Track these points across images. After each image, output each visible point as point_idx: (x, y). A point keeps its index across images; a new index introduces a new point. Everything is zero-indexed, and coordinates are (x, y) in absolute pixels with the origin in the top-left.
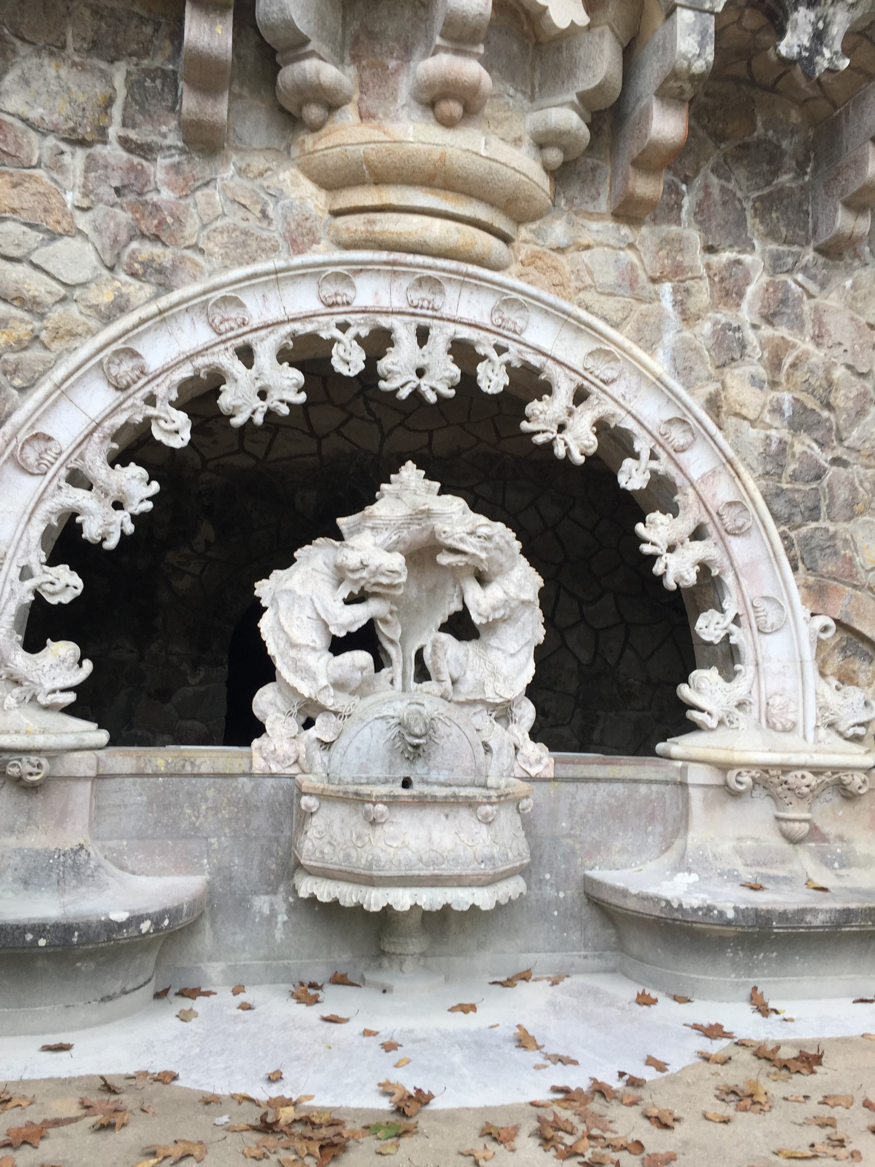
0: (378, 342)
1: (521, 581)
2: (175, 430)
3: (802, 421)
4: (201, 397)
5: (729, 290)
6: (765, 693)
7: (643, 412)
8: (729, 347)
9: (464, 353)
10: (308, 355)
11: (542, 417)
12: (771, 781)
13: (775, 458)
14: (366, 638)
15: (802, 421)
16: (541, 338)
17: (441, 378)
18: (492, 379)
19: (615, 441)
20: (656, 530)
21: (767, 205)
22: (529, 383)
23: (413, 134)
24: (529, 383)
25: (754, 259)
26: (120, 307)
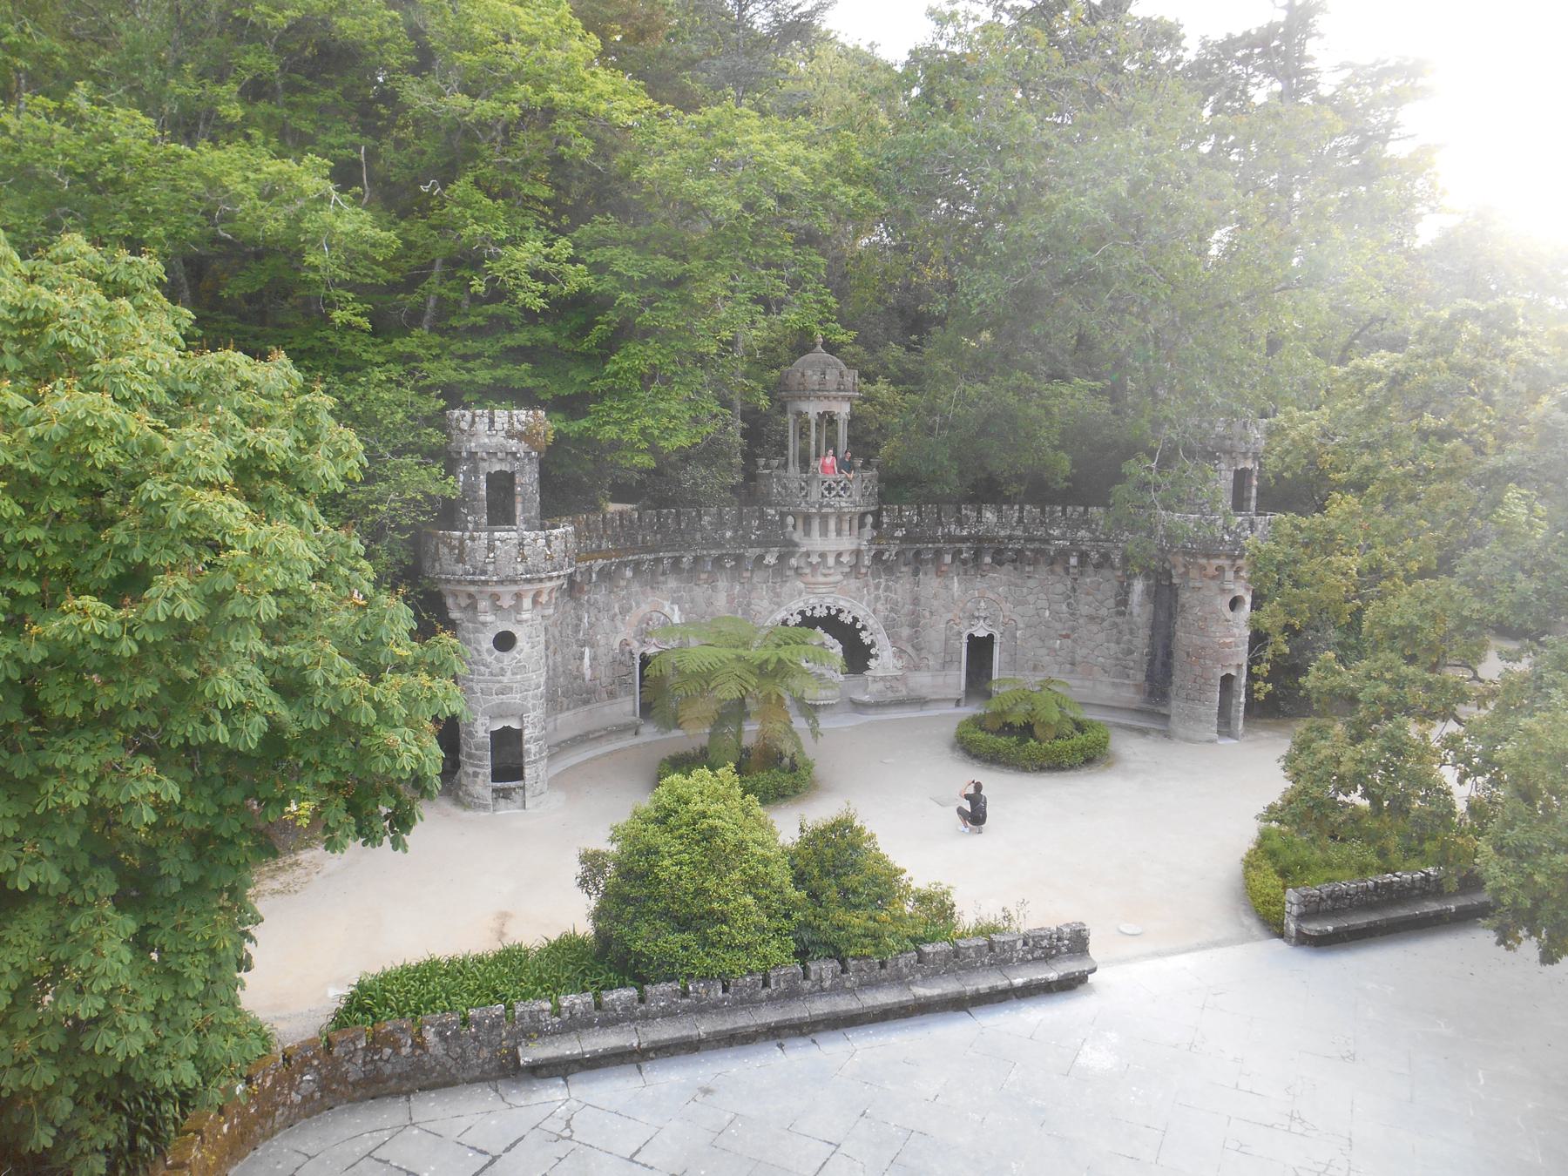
1: (840, 647)
3: (892, 610)
5: (877, 587)
6: (885, 662)
7: (860, 614)
8: (877, 598)
9: (828, 608)
12: (882, 679)
13: (886, 618)
15: (892, 610)
16: (842, 604)
18: (833, 612)
20: (863, 635)
22: (840, 611)
23: (821, 579)
24: (840, 611)
26: (772, 612)
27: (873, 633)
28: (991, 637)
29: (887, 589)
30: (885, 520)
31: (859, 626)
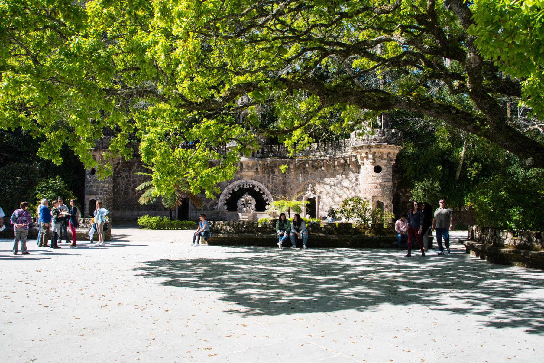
0: (243, 185)
2: (232, 192)
3: (275, 187)
4: (233, 190)
5: (269, 177)
9: (249, 185)
10: (239, 186)
11: (255, 189)
14: (244, 204)
17: (248, 187)
18: (251, 187)
19: (260, 190)
21: (271, 171)
22: (254, 186)
24: (254, 186)
25: (271, 175)
27: (267, 195)
28: (315, 198)
29: (273, 178)
30: (265, 150)
31: (261, 192)
